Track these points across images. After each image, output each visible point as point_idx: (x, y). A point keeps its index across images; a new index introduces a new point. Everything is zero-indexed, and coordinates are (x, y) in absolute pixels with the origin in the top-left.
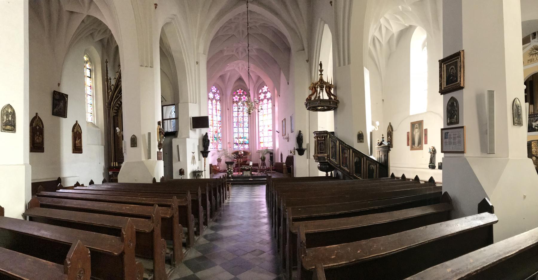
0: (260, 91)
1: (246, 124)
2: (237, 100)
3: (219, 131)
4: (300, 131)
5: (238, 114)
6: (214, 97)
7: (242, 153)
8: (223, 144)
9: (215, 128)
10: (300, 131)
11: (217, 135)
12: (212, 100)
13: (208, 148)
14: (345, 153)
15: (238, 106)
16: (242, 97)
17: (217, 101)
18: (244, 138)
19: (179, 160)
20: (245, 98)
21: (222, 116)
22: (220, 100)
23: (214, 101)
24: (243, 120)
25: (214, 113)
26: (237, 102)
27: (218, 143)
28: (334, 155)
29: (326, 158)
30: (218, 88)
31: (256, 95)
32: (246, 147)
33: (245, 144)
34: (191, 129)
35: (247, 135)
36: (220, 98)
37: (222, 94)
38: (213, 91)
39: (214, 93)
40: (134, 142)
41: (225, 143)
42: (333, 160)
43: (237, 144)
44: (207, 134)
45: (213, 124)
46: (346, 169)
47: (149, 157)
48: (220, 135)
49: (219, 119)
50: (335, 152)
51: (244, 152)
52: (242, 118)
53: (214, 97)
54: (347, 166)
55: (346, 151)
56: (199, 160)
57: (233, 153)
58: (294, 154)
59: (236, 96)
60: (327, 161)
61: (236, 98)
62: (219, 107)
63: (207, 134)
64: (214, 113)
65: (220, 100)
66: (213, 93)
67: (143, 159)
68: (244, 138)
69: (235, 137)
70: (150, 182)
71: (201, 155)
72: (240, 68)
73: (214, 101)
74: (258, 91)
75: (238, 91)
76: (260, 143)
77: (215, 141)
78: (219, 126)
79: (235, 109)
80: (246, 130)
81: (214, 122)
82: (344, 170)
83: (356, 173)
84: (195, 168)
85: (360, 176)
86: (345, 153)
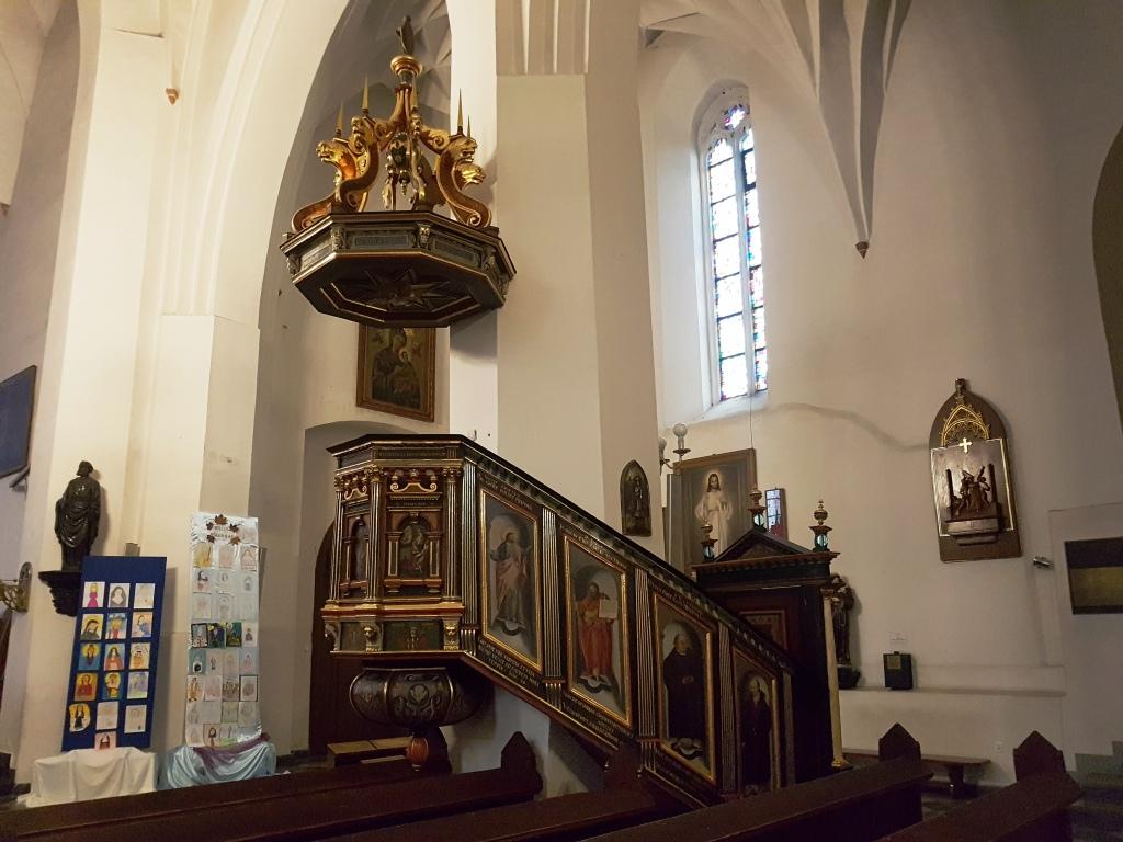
4: (86, 468)
10: (86, 468)
14: (598, 596)
28: (519, 610)
29: (450, 627)
42: (514, 646)
46: (603, 703)
50: (526, 584)
54: (612, 688)
55: (603, 582)
58: (22, 607)
60: (451, 647)
82: (593, 716)
83: (677, 730)
85: (702, 754)
86: (598, 596)
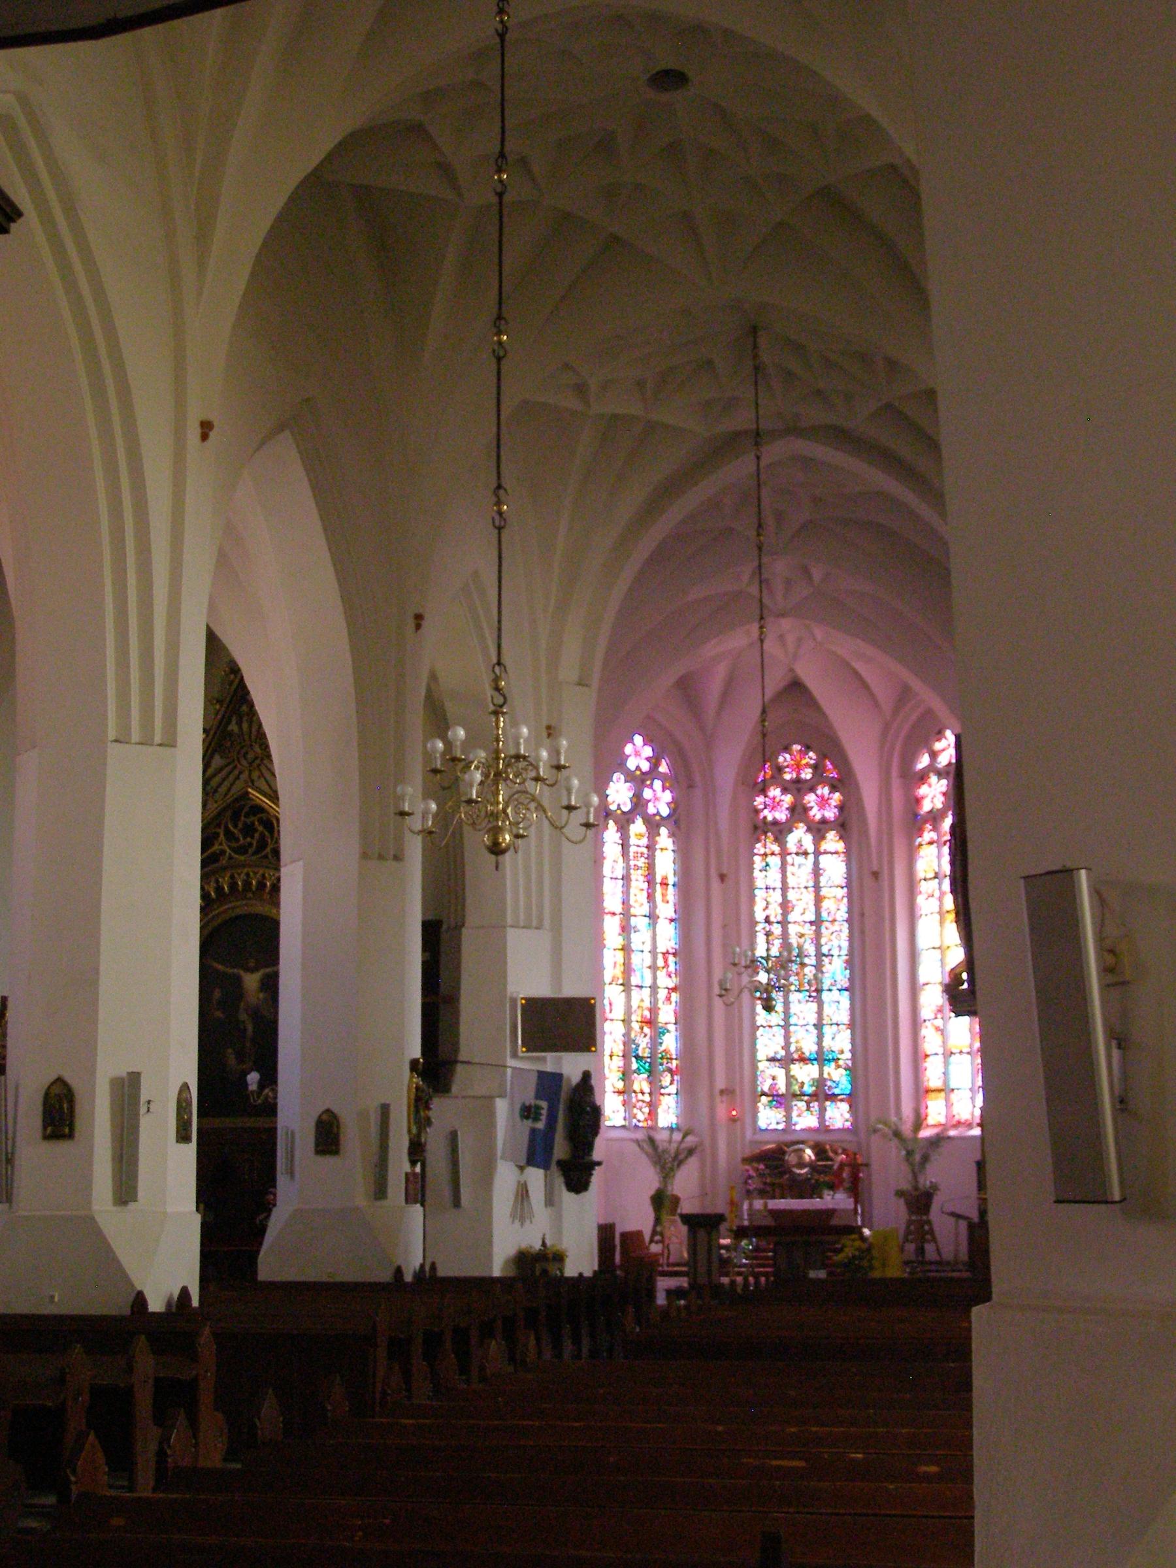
0: (924, 761)
1: (836, 971)
2: (781, 815)
3: (667, 1014)
5: (786, 906)
6: (639, 803)
7: (809, 1153)
8: (688, 1094)
9: (641, 998)
11: (655, 1043)
12: (624, 822)
13: (589, 1146)
15: (784, 853)
16: (810, 799)
17: (653, 824)
18: (821, 1058)
19: (457, 1203)
20: (823, 804)
21: (683, 919)
22: (677, 820)
23: (638, 827)
24: (818, 946)
25: (640, 906)
26: (780, 831)
27: (656, 1090)
30: (662, 746)
31: (896, 782)
32: (839, 1115)
33: (833, 1097)
34: (515, 1055)
35: (840, 1041)
36: (675, 805)
37: (681, 782)
38: (631, 764)
39: (639, 780)
40: (328, 1137)
41: (703, 1094)
43: (780, 1100)
44: (587, 1076)
45: (628, 969)
47: (380, 1191)
48: (670, 1042)
49: (668, 937)
51: (820, 1150)
52: (809, 930)
53: (639, 803)
56: (550, 1201)
57: (745, 1160)
59: (775, 792)
61: (775, 805)
62: (666, 864)
63: (587, 1076)
64: (640, 906)
65: (677, 820)
66: (630, 776)
67: (361, 1200)
68: (821, 1058)
69: (761, 1055)
70: (386, 1276)
71: (559, 1182)
72: (790, 639)
73: (638, 827)
74: (909, 759)
75: (784, 759)
76: (922, 1092)
77: (641, 1083)
78: (665, 982)
79: (766, 875)
80: (838, 1007)
81: (636, 959)
84: (531, 1237)
